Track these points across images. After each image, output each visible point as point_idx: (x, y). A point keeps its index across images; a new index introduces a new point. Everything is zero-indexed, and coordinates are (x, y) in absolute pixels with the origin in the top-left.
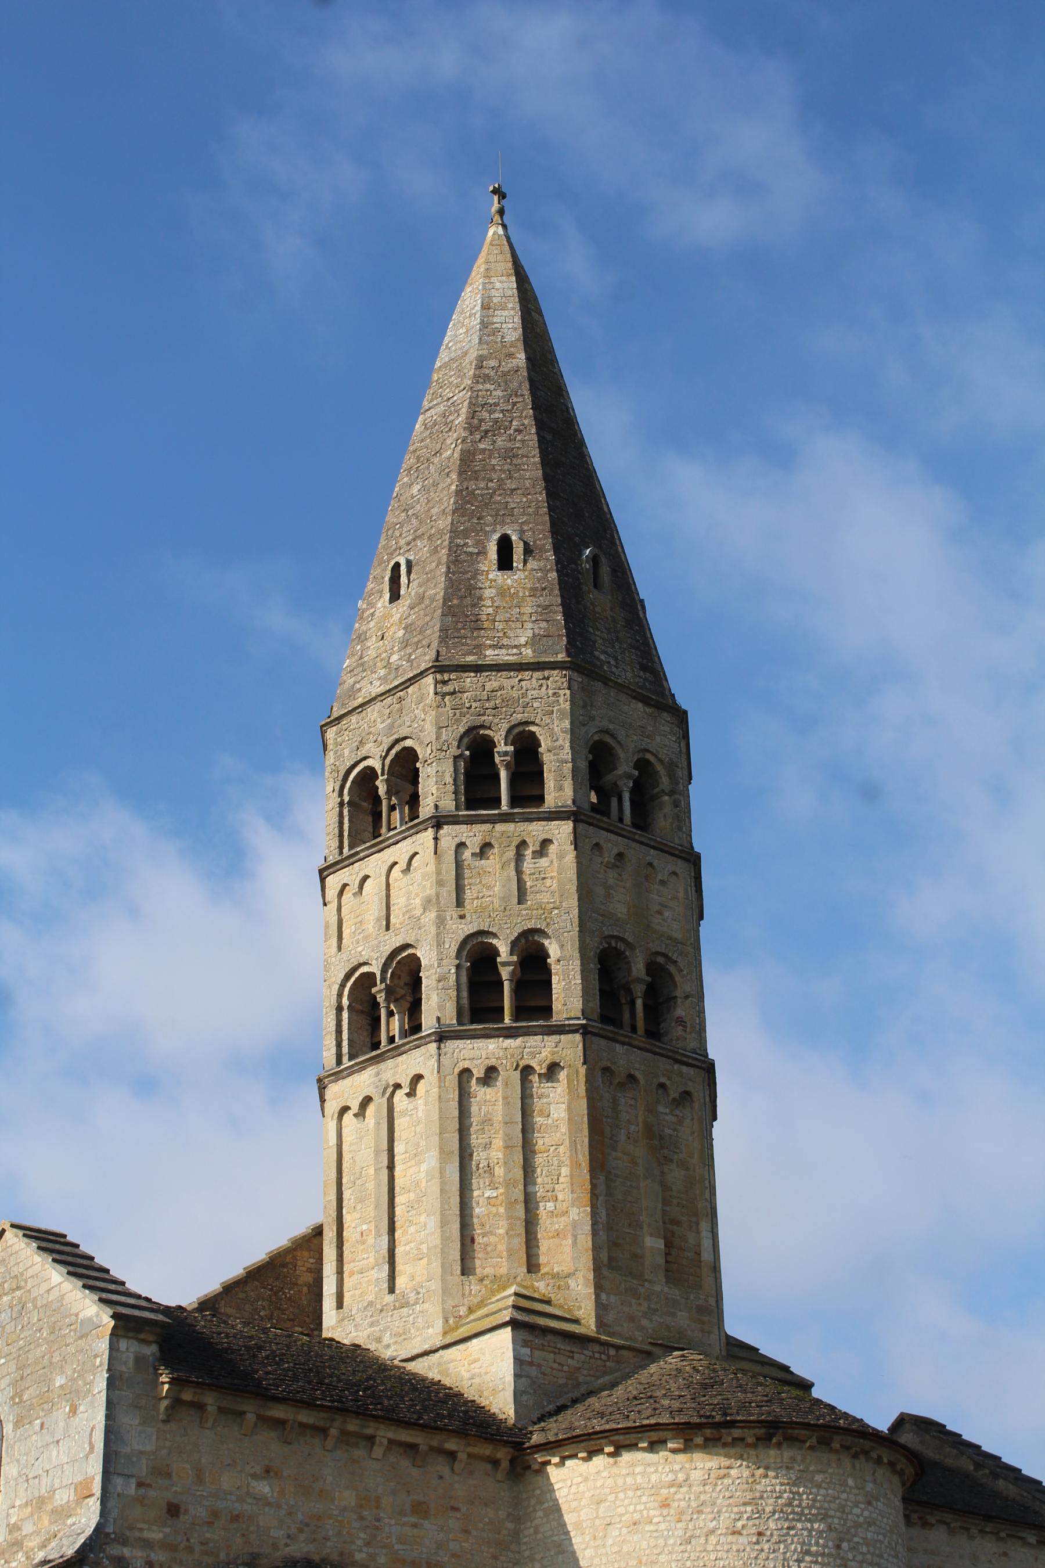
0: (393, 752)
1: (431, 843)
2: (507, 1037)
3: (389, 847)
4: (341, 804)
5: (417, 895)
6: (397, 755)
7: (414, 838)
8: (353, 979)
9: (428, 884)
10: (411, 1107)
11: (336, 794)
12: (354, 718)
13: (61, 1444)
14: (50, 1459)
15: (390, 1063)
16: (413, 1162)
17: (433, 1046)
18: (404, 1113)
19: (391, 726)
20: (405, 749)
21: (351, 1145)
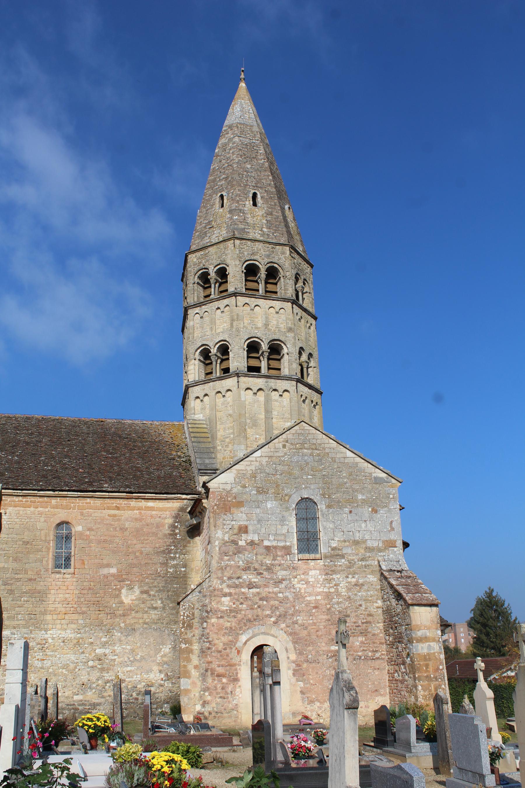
0: (269, 265)
1: (291, 308)
2: (309, 388)
3: (270, 300)
4: (243, 272)
5: (282, 323)
6: (270, 267)
7: (282, 302)
8: (249, 341)
9: (290, 323)
10: (280, 399)
11: (240, 266)
12: (249, 243)
13: (368, 522)
14: (360, 527)
15: (273, 380)
16: (281, 420)
17: (294, 383)
18: (277, 401)
19: (268, 256)
20: (273, 266)
21: (249, 403)
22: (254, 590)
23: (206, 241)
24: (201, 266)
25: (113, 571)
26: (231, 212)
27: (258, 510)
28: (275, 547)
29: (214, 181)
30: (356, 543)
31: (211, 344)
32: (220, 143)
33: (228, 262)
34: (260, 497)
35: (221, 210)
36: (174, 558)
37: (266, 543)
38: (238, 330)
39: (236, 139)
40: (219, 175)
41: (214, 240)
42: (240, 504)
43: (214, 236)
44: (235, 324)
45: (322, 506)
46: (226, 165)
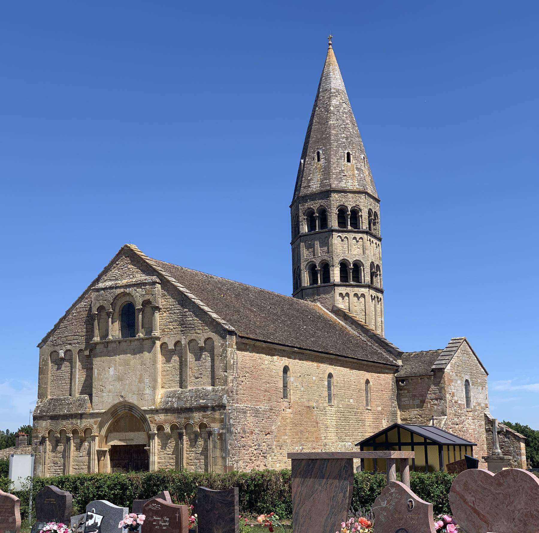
22: (457, 426)
23: (343, 185)
24: (342, 203)
25: (380, 409)
26: (358, 169)
27: (456, 385)
28: (461, 404)
29: (336, 135)
30: (479, 404)
31: (351, 261)
32: (333, 102)
33: (362, 208)
34: (456, 378)
35: (349, 164)
36: (393, 402)
37: (459, 402)
38: (368, 257)
39: (344, 105)
40: (340, 132)
41: (351, 188)
42: (452, 381)
43: (349, 184)
44: (367, 252)
45: (471, 384)
46: (344, 126)
